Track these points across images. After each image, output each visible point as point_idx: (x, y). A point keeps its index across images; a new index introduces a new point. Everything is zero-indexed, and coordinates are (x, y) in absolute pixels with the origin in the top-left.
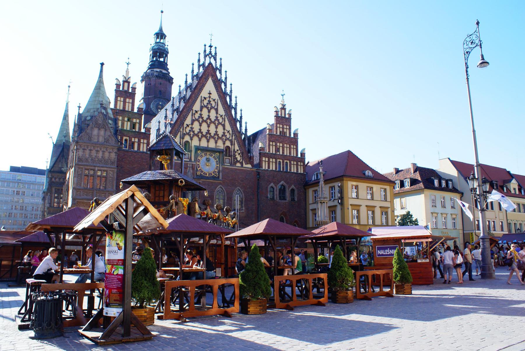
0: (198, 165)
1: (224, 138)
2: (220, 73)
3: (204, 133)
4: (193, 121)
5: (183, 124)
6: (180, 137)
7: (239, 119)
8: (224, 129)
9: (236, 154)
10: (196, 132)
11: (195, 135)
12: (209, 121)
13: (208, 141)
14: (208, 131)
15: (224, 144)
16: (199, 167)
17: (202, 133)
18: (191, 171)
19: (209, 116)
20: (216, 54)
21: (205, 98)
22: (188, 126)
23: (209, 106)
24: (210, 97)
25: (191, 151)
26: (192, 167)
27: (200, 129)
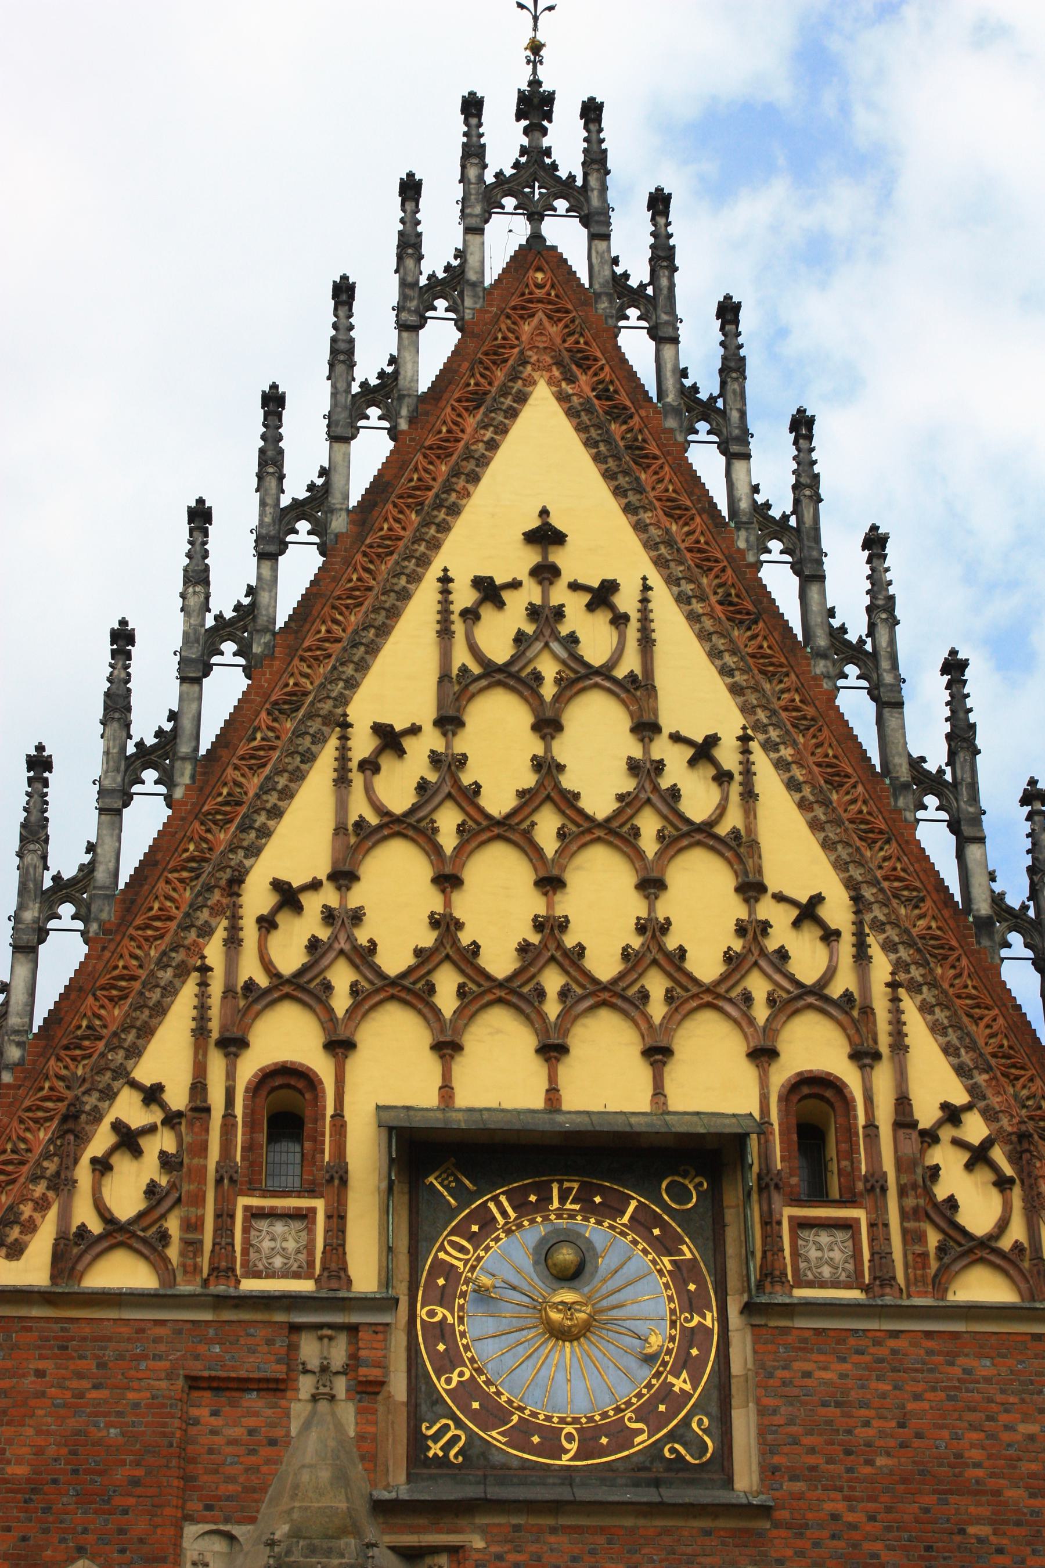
0: (441, 1331)
1: (752, 989)
2: (664, 335)
3: (500, 961)
4: (355, 844)
5: (237, 881)
6: (200, 1032)
7: (936, 758)
8: (751, 889)
9: (947, 1158)
10: (394, 960)
11: (379, 990)
12: (547, 827)
13: (552, 1050)
14: (552, 926)
15: (763, 1055)
16: (449, 1362)
17: (467, 959)
18: (347, 1413)
19: (547, 767)
20: (596, 159)
21: (490, 592)
22: (288, 897)
23: (548, 668)
24: (546, 573)
25: (336, 1180)
26: (354, 1357)
27: (445, 925)
